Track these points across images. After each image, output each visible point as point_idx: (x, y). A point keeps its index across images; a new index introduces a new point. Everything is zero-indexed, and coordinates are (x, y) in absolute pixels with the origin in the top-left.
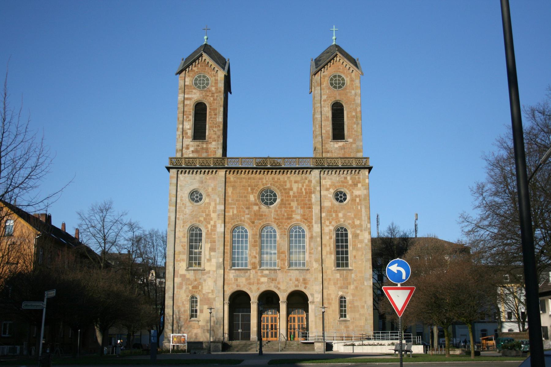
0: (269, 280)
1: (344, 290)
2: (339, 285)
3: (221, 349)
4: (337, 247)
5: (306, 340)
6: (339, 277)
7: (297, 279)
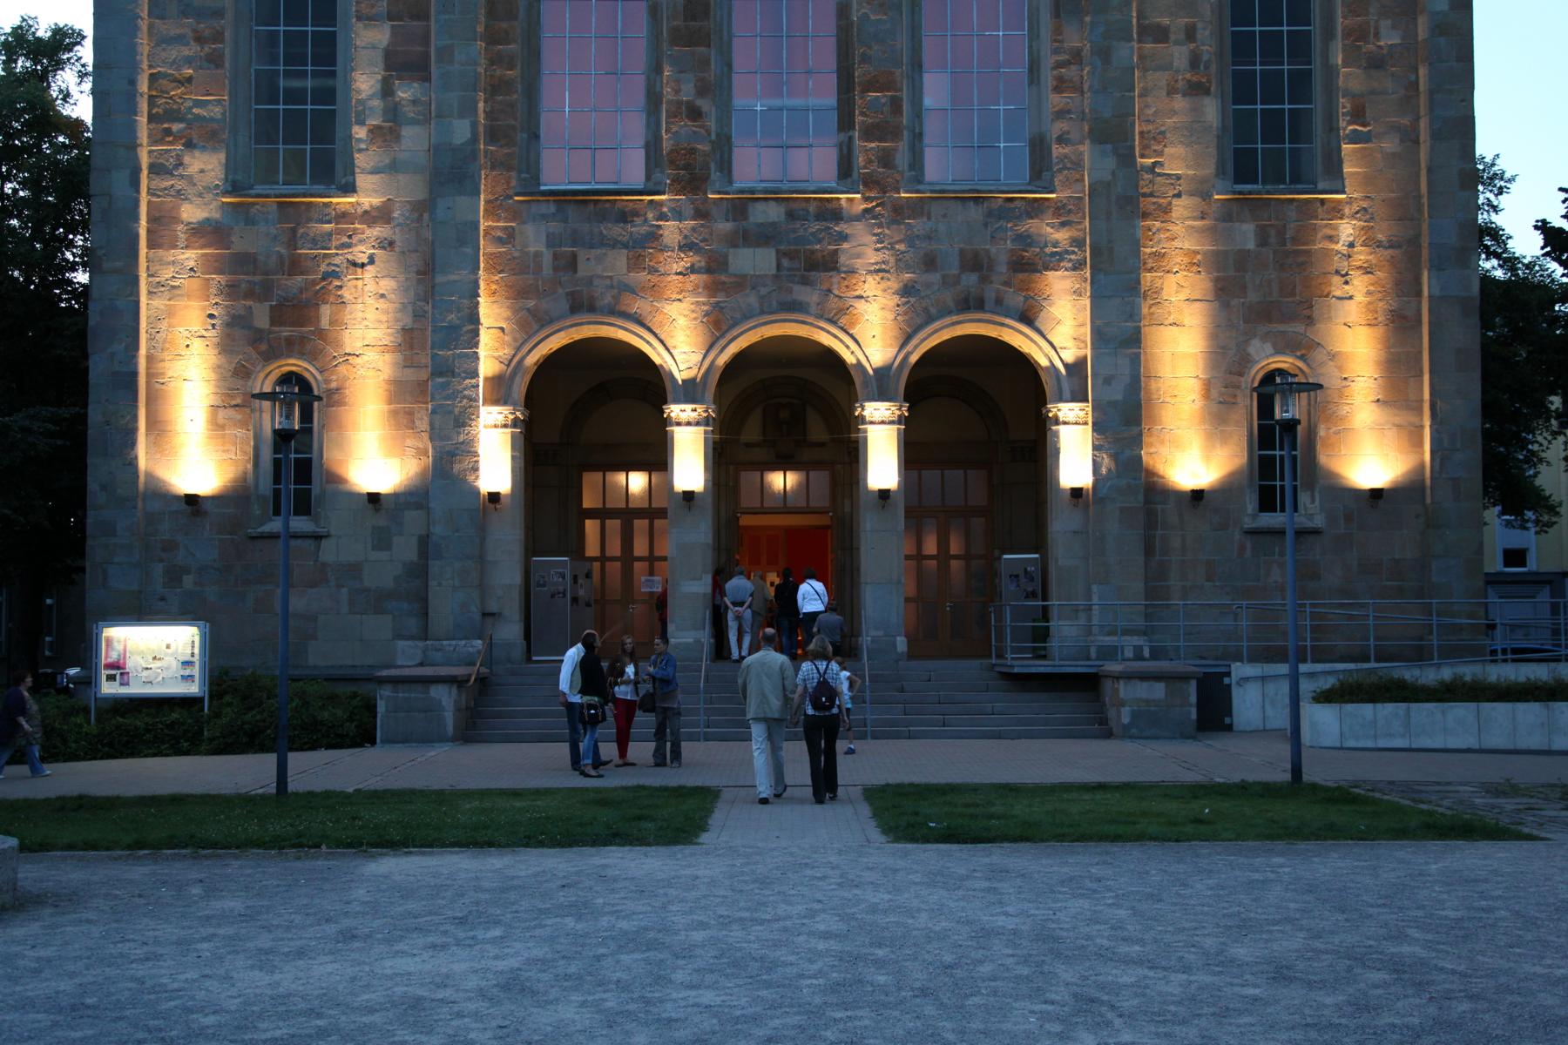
0: (785, 262)
1: (1283, 327)
2: (1253, 296)
3: (450, 728)
4: (1241, 47)
5: (1041, 655)
6: (1251, 246)
7: (976, 254)
